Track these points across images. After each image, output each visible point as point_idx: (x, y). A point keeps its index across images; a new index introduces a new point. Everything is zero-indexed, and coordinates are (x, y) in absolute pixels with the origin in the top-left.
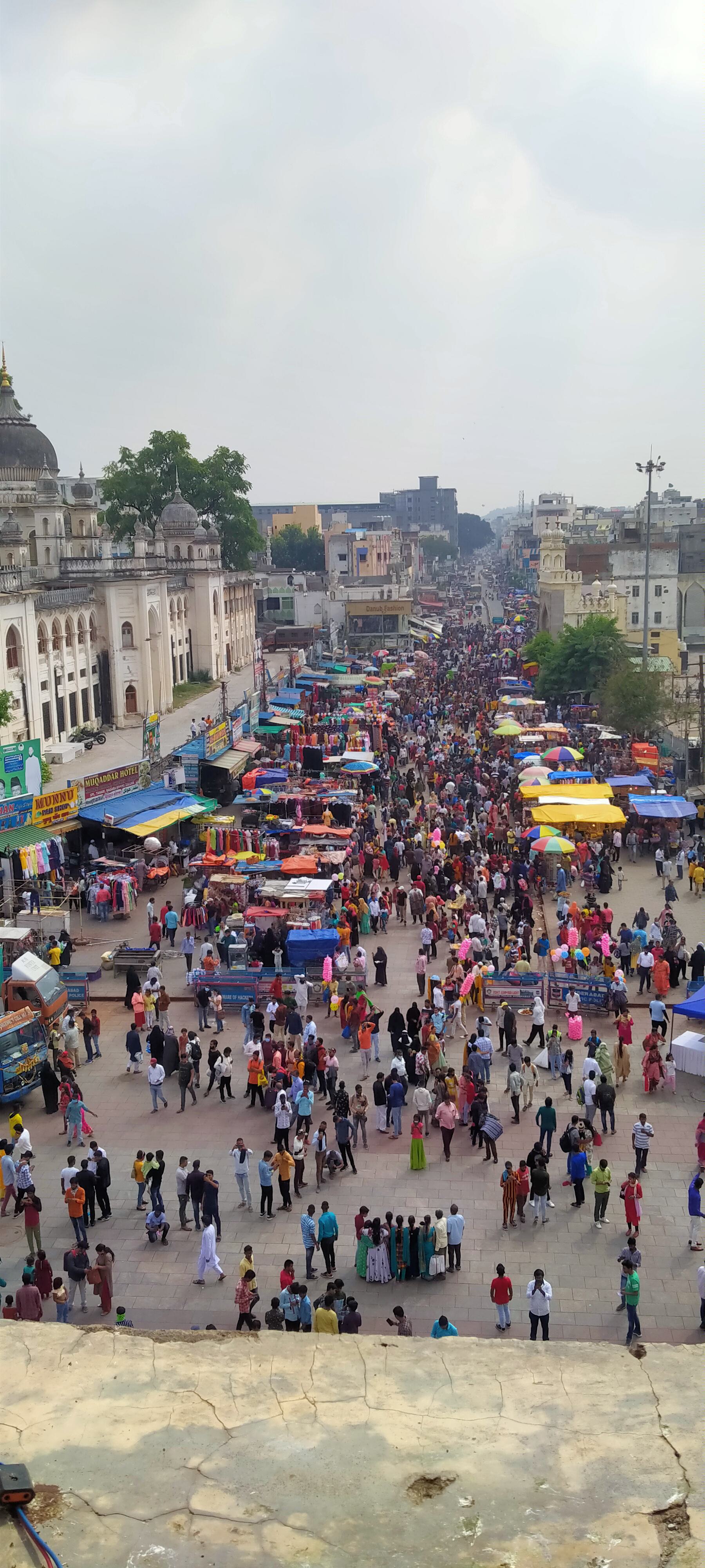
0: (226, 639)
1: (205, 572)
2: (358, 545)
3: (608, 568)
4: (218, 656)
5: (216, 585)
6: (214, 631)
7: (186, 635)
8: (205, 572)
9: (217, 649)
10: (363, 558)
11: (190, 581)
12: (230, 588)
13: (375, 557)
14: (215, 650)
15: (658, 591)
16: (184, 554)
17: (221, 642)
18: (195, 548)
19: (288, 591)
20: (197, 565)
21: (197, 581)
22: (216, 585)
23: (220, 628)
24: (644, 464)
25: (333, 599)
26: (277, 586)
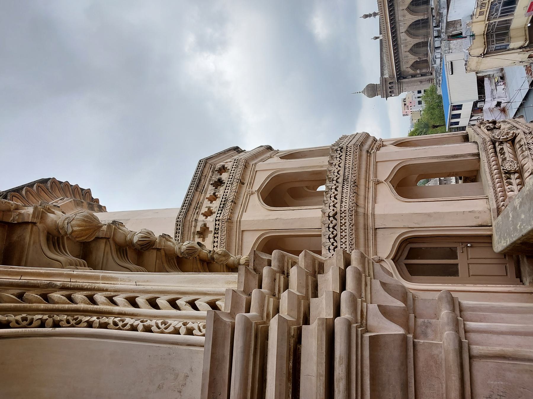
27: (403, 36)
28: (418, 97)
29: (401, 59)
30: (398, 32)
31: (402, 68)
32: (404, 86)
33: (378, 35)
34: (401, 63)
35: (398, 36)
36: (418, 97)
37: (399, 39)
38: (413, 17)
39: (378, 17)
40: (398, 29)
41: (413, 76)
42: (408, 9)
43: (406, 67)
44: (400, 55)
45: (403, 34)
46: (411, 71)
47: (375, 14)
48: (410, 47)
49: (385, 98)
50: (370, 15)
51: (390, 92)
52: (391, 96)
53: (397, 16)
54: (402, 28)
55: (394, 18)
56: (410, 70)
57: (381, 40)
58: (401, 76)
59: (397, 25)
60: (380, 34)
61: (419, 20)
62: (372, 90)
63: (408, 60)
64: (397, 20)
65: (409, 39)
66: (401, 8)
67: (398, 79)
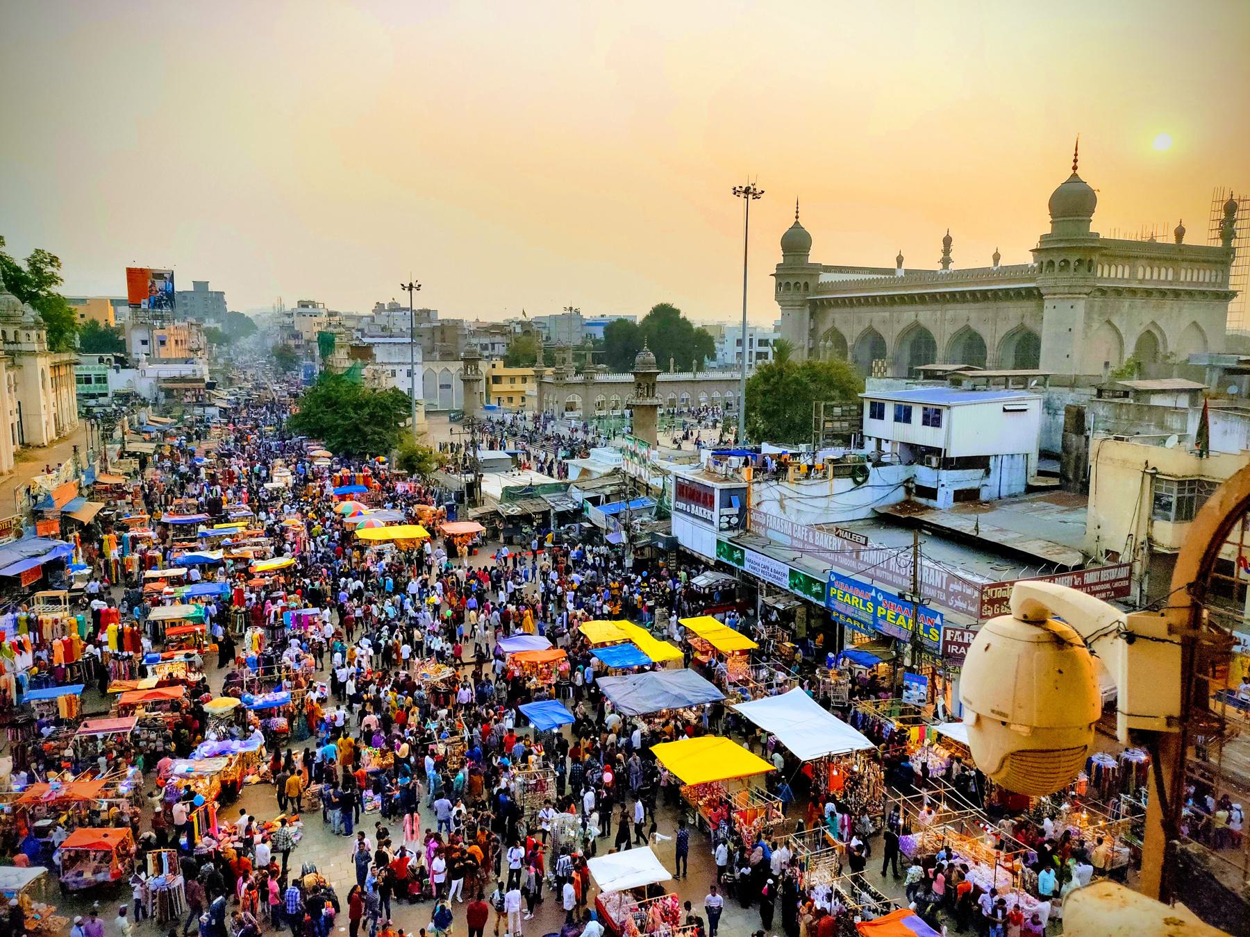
0: (53, 410)
1: (33, 353)
2: (158, 333)
3: (372, 356)
4: (47, 423)
5: (44, 363)
6: (43, 403)
7: (17, 406)
8: (33, 353)
9: (46, 417)
10: (163, 343)
11: (17, 360)
12: (55, 367)
13: (173, 343)
14: (44, 419)
15: (410, 374)
16: (11, 338)
17: (49, 413)
18: (23, 334)
19: (100, 369)
20: (24, 347)
21: (25, 360)
22: (44, 363)
23: (48, 401)
24: (407, 285)
25: (144, 375)
26: (91, 365)
27: (908, 315)
28: (751, 340)
29: (856, 310)
30: (920, 307)
31: (836, 310)
32: (795, 314)
33: (904, 266)
35: (911, 308)
36: (751, 340)
39: (938, 267)
40: (929, 307)
41: (813, 333)
42: (967, 329)
43: (835, 318)
44: (863, 309)
46: (823, 329)
47: (946, 261)
48: (881, 329)
50: (947, 251)
52: (779, 285)
53: (959, 306)
54: (926, 316)
56: (828, 326)
57: (892, 271)
58: (817, 308)
59: (935, 307)
61: (935, 348)
63: (851, 325)
64: (949, 306)
65: (899, 328)
66: (973, 315)
67: (813, 302)
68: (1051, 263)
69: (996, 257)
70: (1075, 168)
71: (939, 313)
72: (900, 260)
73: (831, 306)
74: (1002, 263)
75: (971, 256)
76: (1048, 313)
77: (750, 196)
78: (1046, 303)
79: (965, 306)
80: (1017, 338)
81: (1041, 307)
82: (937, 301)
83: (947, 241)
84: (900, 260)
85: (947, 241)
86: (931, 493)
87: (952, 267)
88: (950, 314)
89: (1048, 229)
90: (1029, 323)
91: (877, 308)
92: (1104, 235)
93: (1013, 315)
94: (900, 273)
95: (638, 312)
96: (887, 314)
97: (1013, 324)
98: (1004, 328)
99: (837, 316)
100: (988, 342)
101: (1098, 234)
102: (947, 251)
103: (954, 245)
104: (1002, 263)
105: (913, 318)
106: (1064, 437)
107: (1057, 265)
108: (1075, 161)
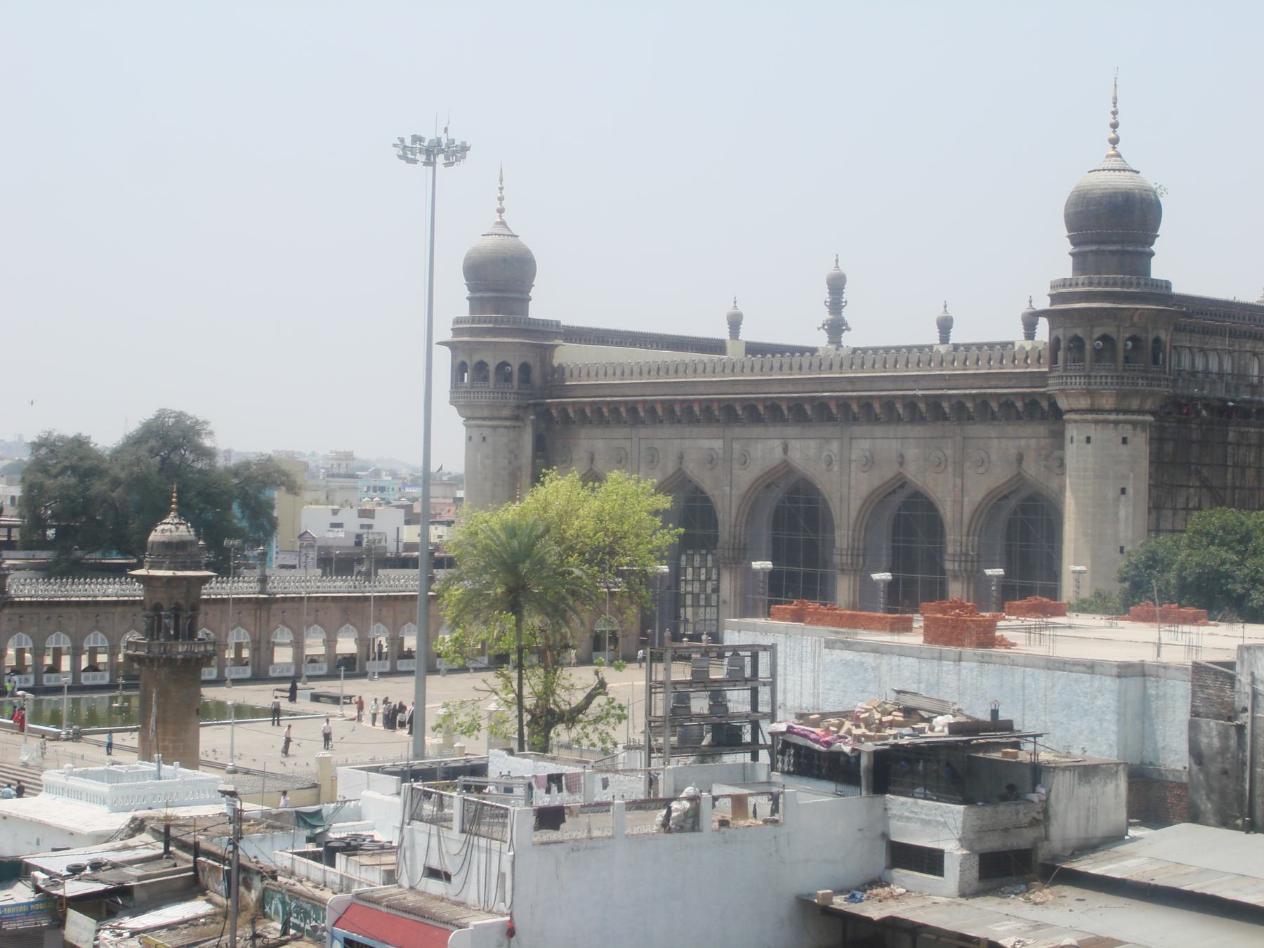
27: (767, 449)
29: (644, 432)
30: (791, 431)
34: (625, 431)
37: (757, 431)
38: (856, 505)
39: (820, 340)
42: (901, 483)
44: (666, 431)
45: (778, 454)
47: (836, 328)
48: (705, 480)
49: (448, 336)
50: (836, 304)
51: (481, 366)
53: (878, 431)
54: (806, 451)
55: (873, 419)
57: (716, 347)
59: (828, 430)
60: (754, 349)
62: (500, 280)
64: (857, 430)
65: (745, 478)
66: (912, 452)
68: (1077, 344)
69: (945, 326)
70: (1114, 142)
71: (835, 446)
72: (735, 323)
73: (584, 420)
74: (956, 337)
75: (890, 322)
76: (1075, 453)
77: (441, 159)
78: (1072, 431)
79: (891, 430)
80: (1013, 502)
81: (1058, 438)
82: (830, 419)
83: (836, 286)
84: (735, 323)
85: (836, 286)
86: (929, 861)
87: (849, 340)
88: (861, 447)
89: (1064, 268)
90: (1032, 469)
91: (695, 431)
92: (1180, 287)
93: (1001, 452)
94: (735, 353)
95: (108, 432)
96: (718, 444)
97: (999, 475)
98: (979, 486)
99: (600, 445)
100: (948, 512)
101: (1167, 285)
102: (836, 304)
103: (847, 294)
104: (956, 337)
105: (778, 454)
106: (1193, 727)
107: (1088, 347)
108: (1115, 126)
